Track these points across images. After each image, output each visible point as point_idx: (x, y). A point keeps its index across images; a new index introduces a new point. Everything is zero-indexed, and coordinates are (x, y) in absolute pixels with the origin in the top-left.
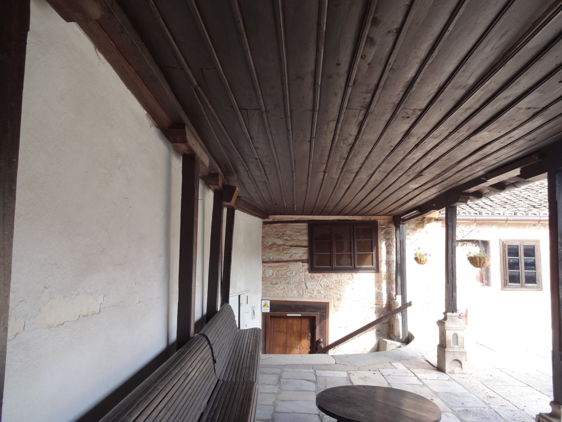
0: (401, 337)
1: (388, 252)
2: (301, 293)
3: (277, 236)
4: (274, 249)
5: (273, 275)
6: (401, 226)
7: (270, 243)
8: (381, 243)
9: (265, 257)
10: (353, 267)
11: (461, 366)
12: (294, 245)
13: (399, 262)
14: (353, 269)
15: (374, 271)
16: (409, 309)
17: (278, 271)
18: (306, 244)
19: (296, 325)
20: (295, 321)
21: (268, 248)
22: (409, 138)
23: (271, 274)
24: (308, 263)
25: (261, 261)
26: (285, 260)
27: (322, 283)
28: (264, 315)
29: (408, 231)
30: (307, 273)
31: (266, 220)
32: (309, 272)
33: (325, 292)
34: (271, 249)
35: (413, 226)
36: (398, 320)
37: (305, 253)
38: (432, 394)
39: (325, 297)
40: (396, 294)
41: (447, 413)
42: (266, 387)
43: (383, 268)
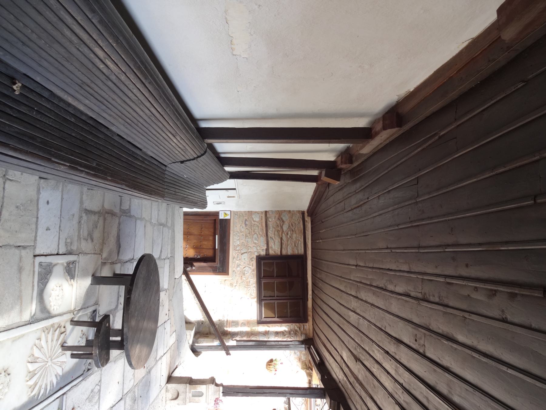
0: (196, 345)
1: (277, 333)
3: (290, 224)
4: (278, 222)
5: (254, 221)
6: (303, 346)
7: (284, 218)
8: (286, 326)
9: (271, 213)
10: (263, 298)
11: (173, 399)
13: (268, 343)
14: (261, 299)
15: (259, 319)
16: (223, 352)
17: (258, 227)
18: (284, 253)
19: (207, 244)
20: (211, 243)
21: (280, 216)
22: (394, 344)
23: (254, 219)
25: (267, 210)
26: (269, 233)
28: (217, 214)
29: (298, 353)
30: (256, 254)
31: (306, 214)
32: (257, 256)
33: (238, 271)
34: (279, 219)
35: (303, 358)
36: (213, 342)
38: (149, 368)
39: (234, 271)
40: (237, 341)
41: (133, 381)
42: (156, 212)
43: (262, 328)
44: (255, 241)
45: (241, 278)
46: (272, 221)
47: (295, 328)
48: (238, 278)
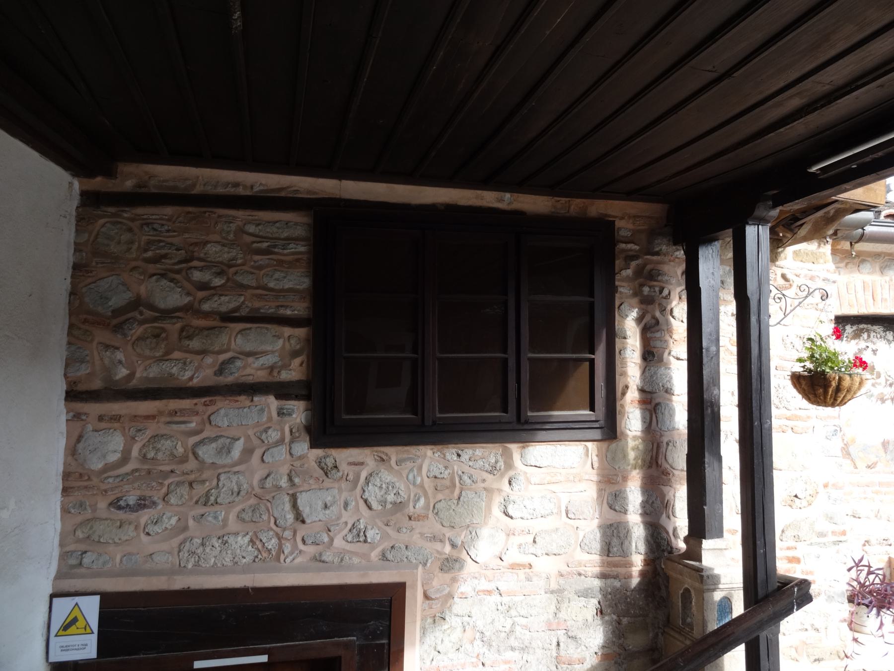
1: (652, 355)
2: (272, 544)
3: (152, 268)
5: (125, 458)
7: (118, 300)
9: (83, 370)
10: (511, 416)
12: (244, 312)
15: (597, 434)
17: (155, 438)
18: (299, 308)
23: (114, 458)
24: (307, 398)
25: (61, 387)
27: (373, 494)
30: (302, 447)
31: (98, 183)
32: (313, 445)
33: (385, 536)
34: (118, 328)
37: (295, 354)
39: (384, 557)
43: (632, 422)
44: (236, 453)
45: (419, 518)
46: (128, 363)
47: (627, 279)
48: (416, 537)
